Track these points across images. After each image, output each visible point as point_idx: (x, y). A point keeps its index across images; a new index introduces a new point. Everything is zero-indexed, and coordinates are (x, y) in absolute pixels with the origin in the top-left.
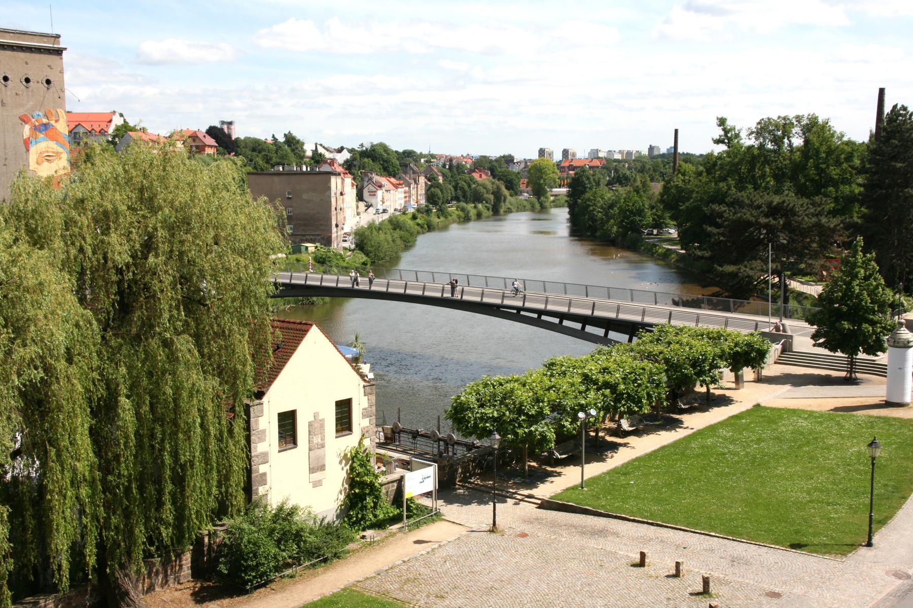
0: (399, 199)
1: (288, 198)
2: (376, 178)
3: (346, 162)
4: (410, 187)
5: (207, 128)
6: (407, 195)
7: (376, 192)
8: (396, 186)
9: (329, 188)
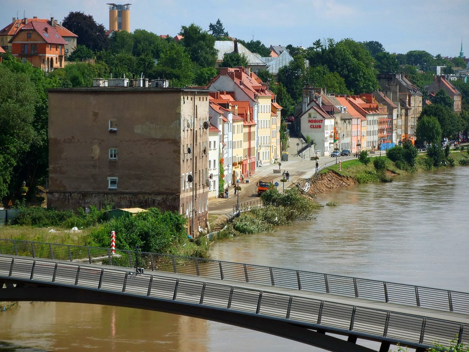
0: (369, 133)
1: (112, 132)
2: (324, 97)
3: (284, 71)
4: (391, 114)
5: (67, 15)
6: (385, 126)
7: (321, 121)
8: (363, 113)
9: (178, 116)
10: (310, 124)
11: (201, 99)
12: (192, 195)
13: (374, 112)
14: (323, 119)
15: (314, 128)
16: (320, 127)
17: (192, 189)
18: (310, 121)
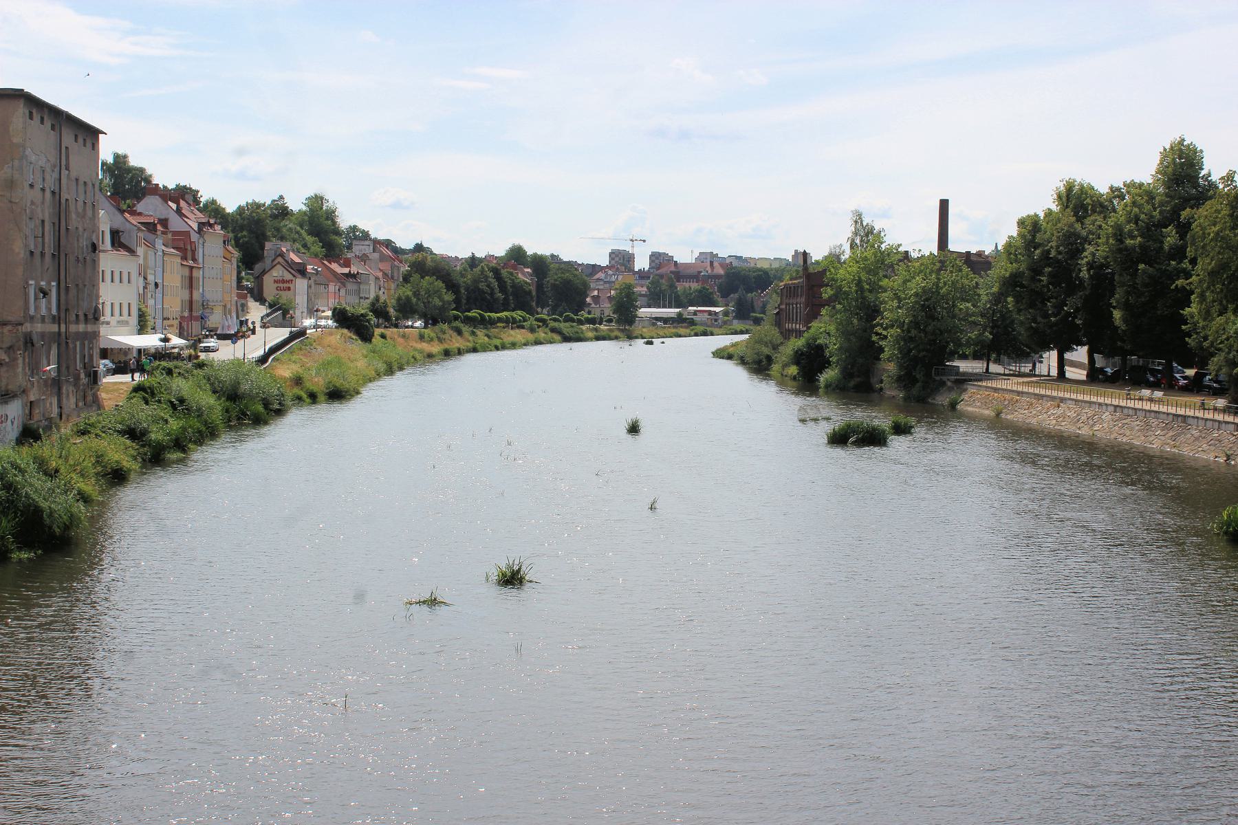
10: (276, 285)
11: (80, 140)
12: (57, 330)
13: (355, 280)
14: (294, 279)
15: (281, 290)
16: (289, 289)
17: (57, 318)
18: (276, 282)
